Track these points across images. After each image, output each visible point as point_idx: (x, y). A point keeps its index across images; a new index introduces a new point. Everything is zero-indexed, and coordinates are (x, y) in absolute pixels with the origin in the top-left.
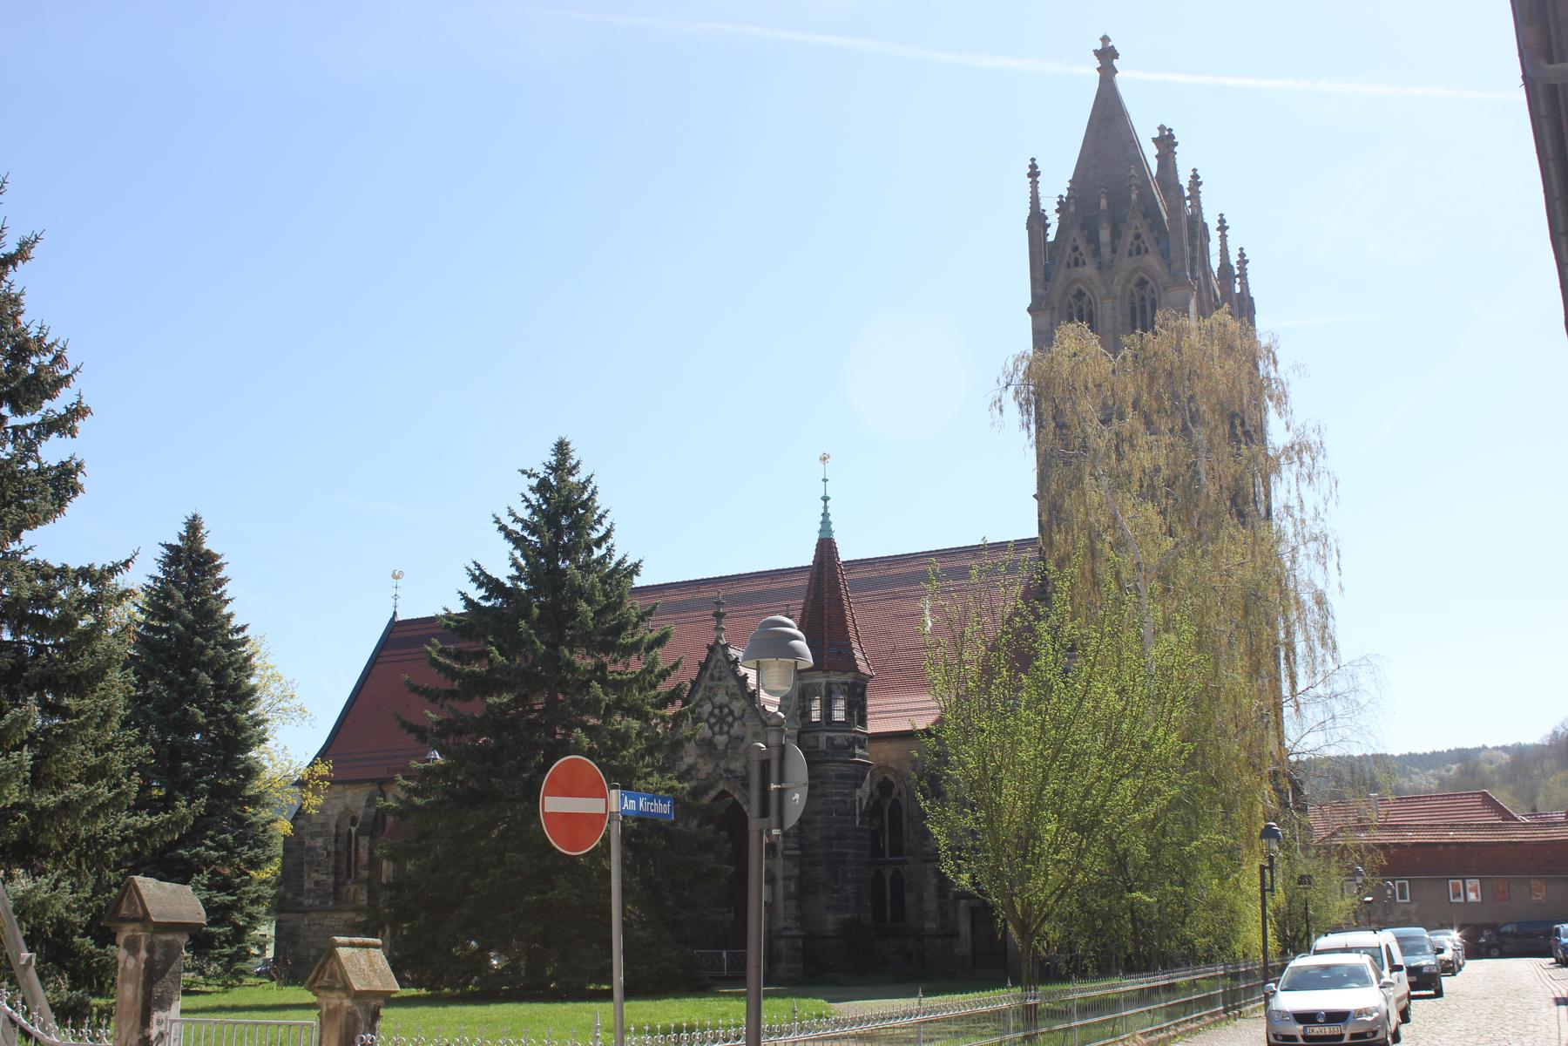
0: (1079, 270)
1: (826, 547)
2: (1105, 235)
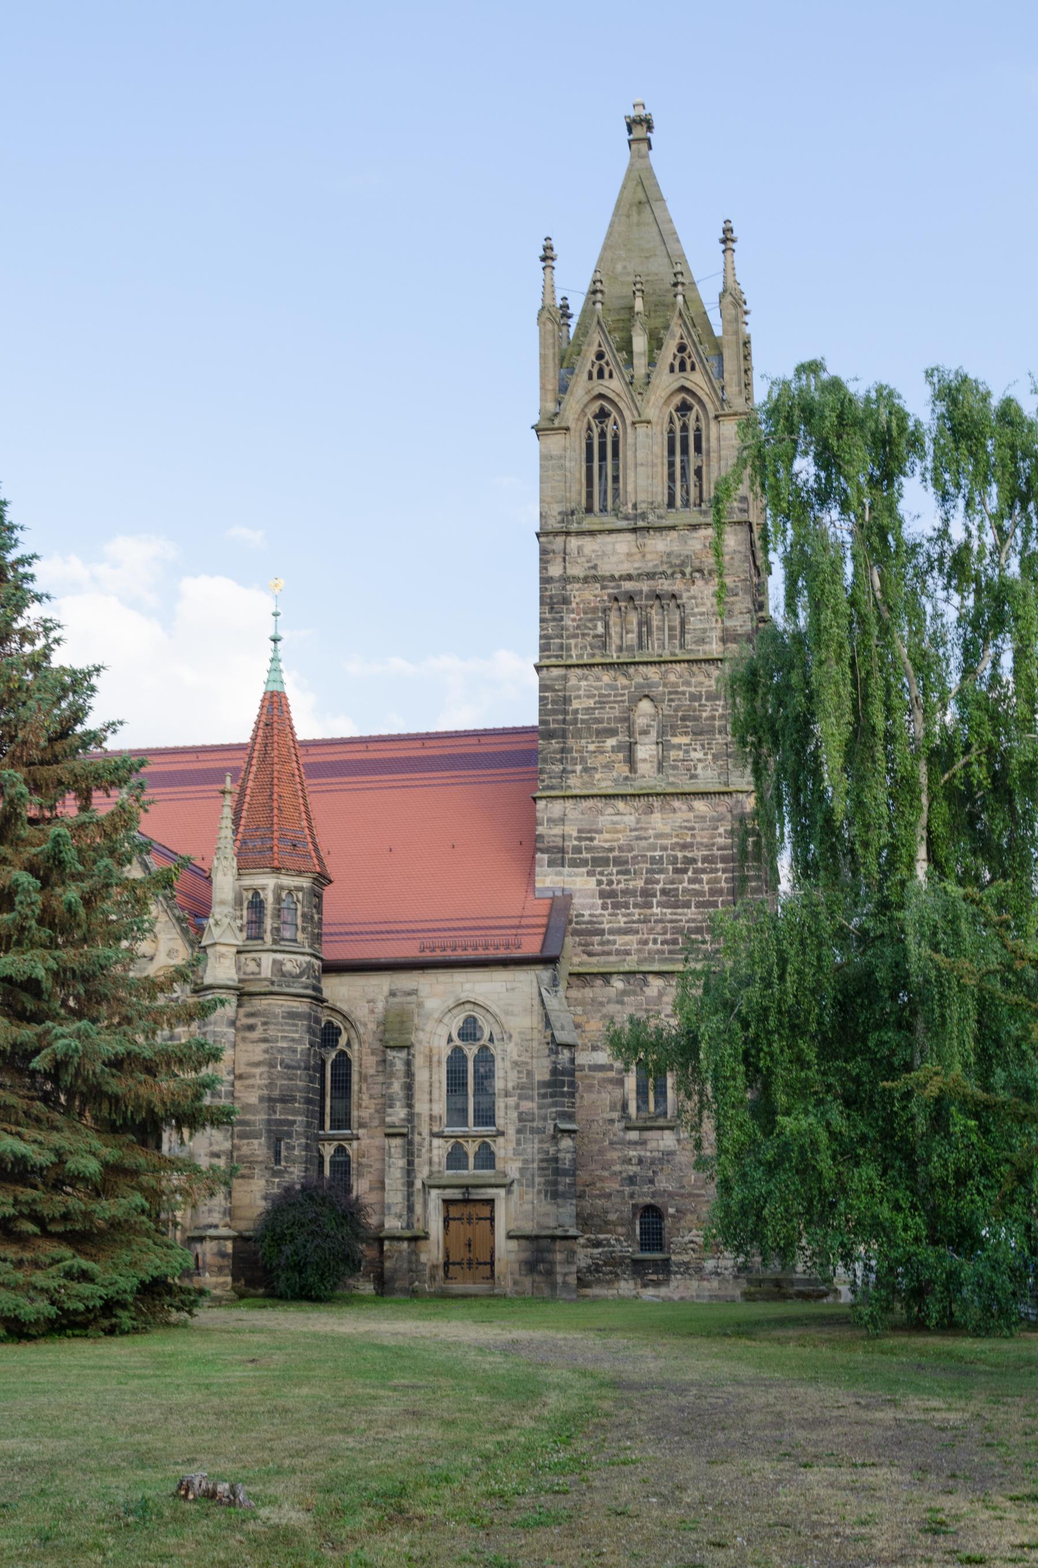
0: (606, 382)
1: (274, 708)
2: (640, 343)
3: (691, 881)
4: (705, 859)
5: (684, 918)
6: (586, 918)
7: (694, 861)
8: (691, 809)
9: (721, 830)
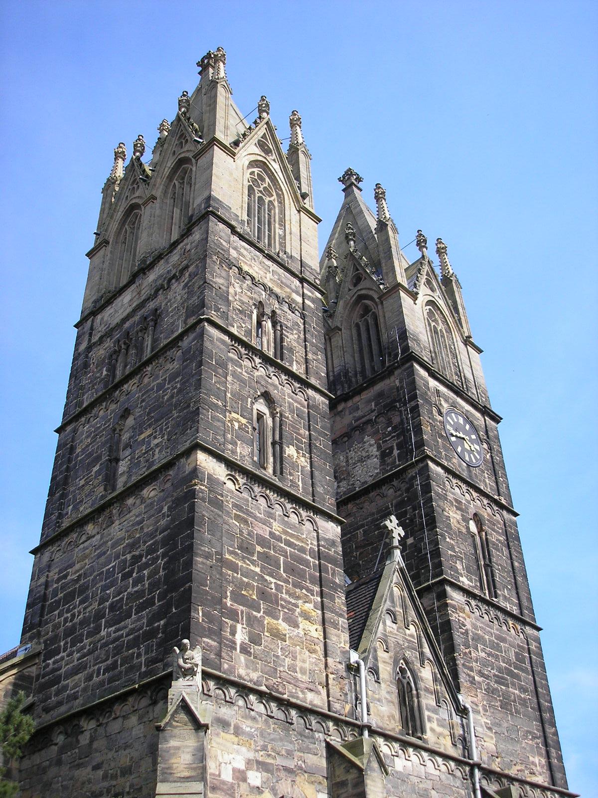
3: (135, 584)
4: (151, 550)
5: (124, 632)
6: (51, 667)
7: (141, 556)
8: (143, 501)
9: (165, 509)
